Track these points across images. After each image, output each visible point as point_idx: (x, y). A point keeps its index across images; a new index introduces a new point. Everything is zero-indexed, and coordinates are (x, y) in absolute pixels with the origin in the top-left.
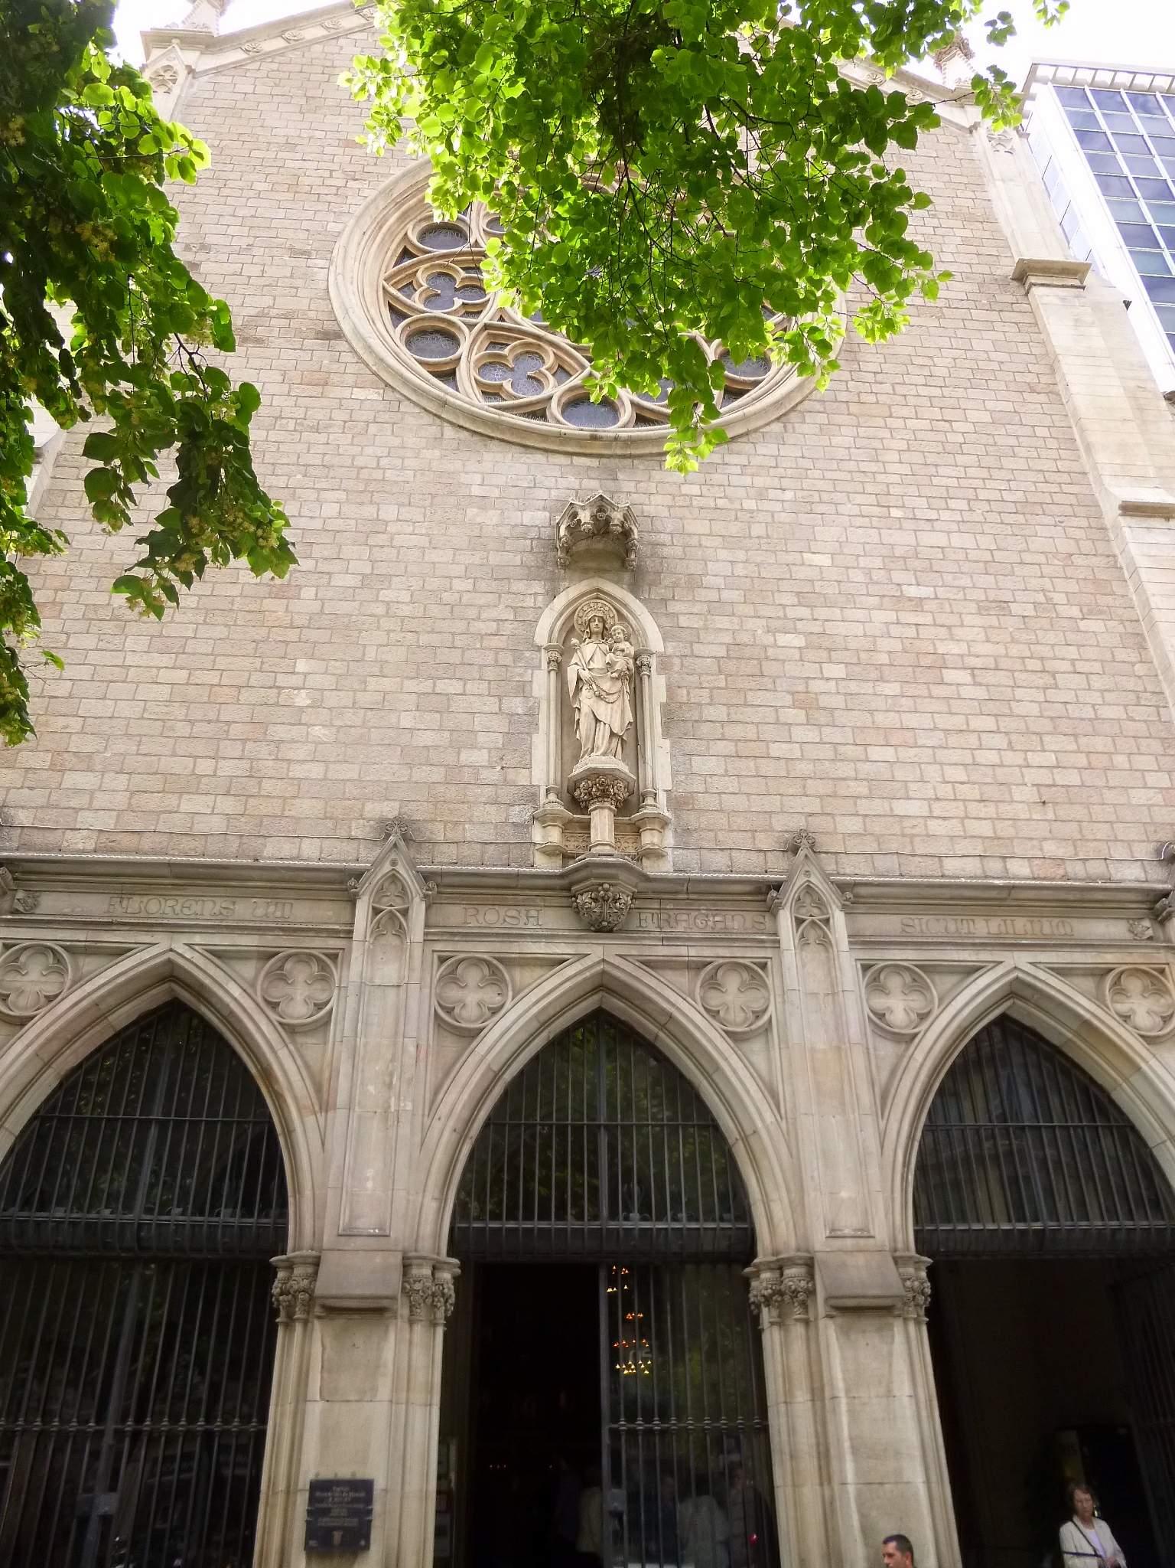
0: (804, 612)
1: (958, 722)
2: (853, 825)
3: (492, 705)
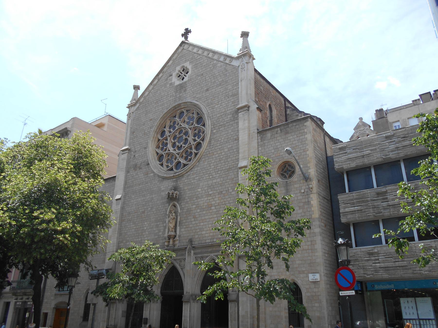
0: (196, 201)
1: (212, 216)
2: (197, 236)
3: (162, 225)
